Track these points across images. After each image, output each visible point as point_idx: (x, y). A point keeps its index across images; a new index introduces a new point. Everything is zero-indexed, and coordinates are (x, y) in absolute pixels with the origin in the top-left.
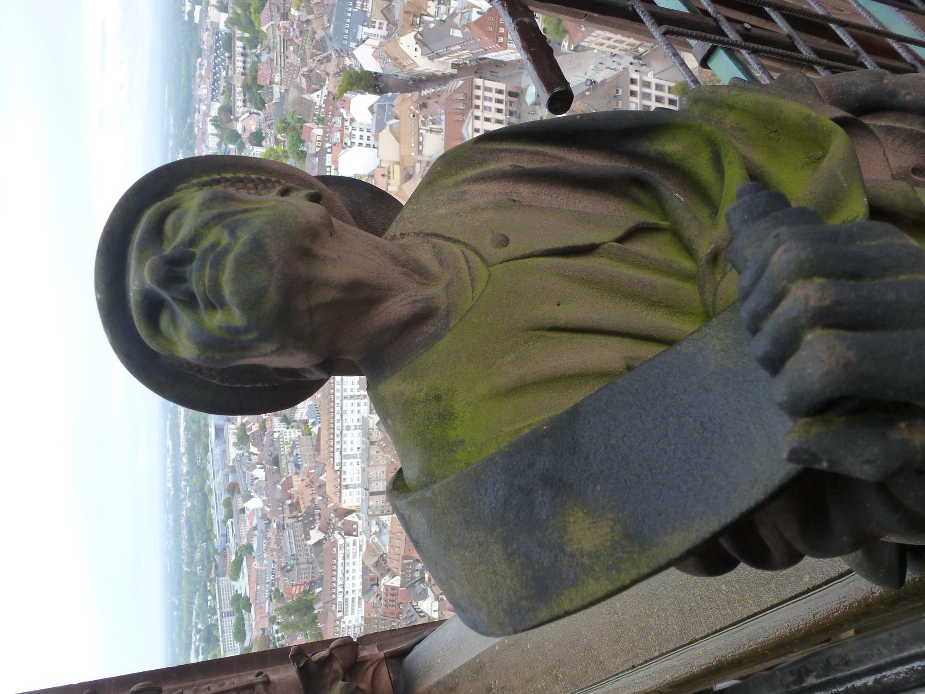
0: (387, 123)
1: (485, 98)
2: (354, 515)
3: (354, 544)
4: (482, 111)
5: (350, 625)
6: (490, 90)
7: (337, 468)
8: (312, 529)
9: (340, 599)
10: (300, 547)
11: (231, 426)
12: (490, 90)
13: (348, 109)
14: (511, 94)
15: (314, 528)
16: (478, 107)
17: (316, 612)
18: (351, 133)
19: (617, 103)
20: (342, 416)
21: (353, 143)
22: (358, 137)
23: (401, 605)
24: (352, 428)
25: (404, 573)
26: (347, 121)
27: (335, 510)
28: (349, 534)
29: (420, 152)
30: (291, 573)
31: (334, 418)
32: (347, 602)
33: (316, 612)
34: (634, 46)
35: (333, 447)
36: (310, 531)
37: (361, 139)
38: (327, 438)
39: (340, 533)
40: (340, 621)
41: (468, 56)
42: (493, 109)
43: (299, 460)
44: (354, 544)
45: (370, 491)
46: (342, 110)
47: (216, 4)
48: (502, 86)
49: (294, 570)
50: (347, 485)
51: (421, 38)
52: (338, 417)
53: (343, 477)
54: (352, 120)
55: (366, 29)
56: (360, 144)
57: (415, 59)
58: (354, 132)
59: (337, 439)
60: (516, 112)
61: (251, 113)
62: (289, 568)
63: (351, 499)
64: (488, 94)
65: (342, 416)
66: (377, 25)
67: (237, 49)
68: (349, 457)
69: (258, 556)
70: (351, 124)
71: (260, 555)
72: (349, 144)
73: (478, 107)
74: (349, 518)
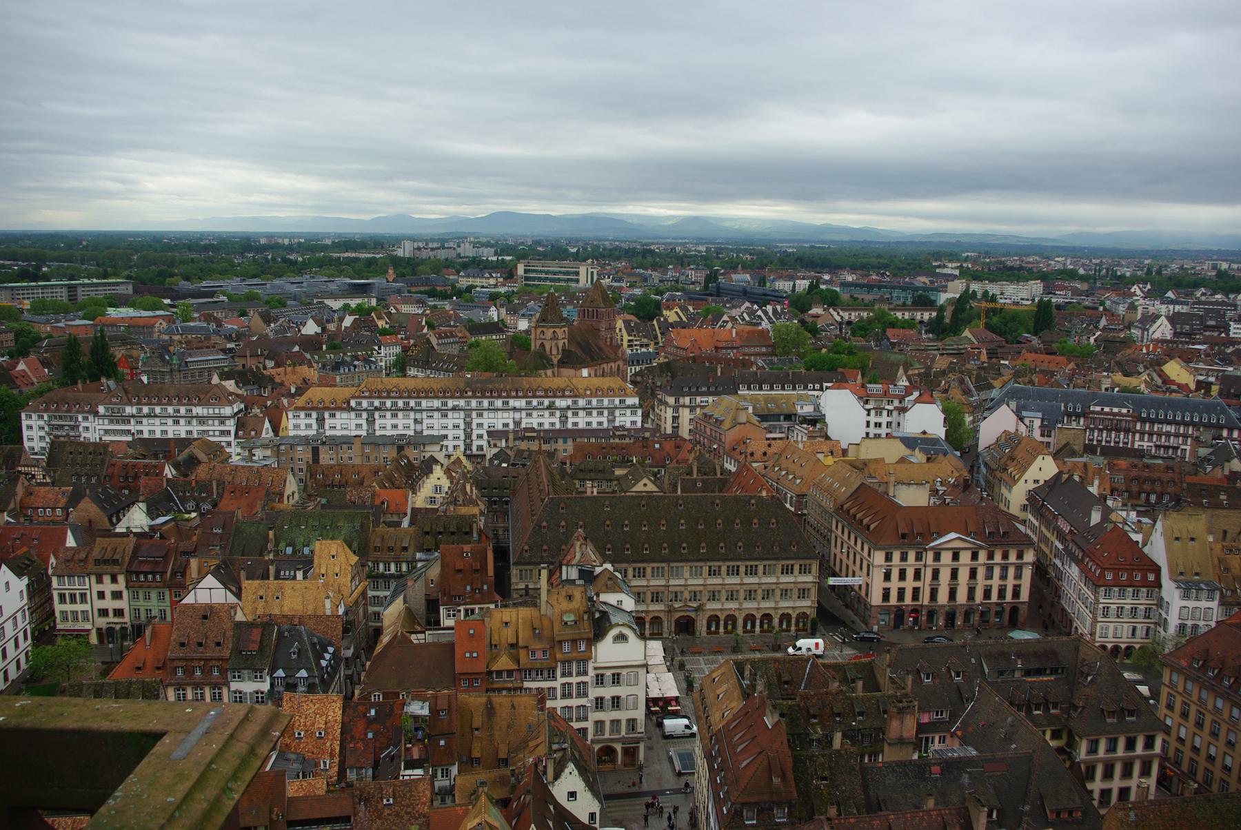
0: (917, 450)
1: (1004, 568)
2: (271, 434)
3: (223, 433)
4: (985, 564)
5: (81, 429)
6: (1018, 576)
7: (353, 403)
8: (237, 384)
9: (129, 410)
10: (200, 376)
11: (374, 302)
12: (1018, 576)
13: (917, 401)
14: (1014, 610)
15: (238, 386)
16: (991, 557)
17: (103, 380)
18: (884, 409)
19: (1114, 712)
20: (438, 410)
21: (868, 415)
22: (878, 420)
23: (126, 492)
24: (419, 428)
25: (194, 485)
26: (900, 402)
27: (277, 407)
28: (240, 426)
29: (898, 483)
30: (157, 360)
31: (436, 397)
32: (123, 422)
33: (103, 380)
34: (1176, 762)
35: (388, 397)
36: (232, 382)
37: (876, 424)
38: (402, 387)
39: (240, 411)
40: (89, 412)
41: (1047, 551)
42: (989, 582)
43: (347, 370)
44: (223, 433)
45: (321, 447)
46: (916, 394)
47: (971, 290)
48: (1025, 596)
49: (163, 366)
50: (324, 419)
51: (1063, 480)
52: (437, 403)
53: (338, 414)
54: (903, 410)
55: (1037, 423)
56: (868, 423)
57: (1023, 480)
58: (885, 413)
59: (400, 403)
60: (988, 622)
61: (840, 324)
62: (167, 357)
63: (298, 425)
64: (1011, 572)
65: (438, 410)
66: (1046, 439)
67: (919, 314)
68: (371, 422)
69: (177, 328)
70: (896, 408)
71: (178, 330)
72: (868, 407)
73: (991, 557)
74: (267, 424)
